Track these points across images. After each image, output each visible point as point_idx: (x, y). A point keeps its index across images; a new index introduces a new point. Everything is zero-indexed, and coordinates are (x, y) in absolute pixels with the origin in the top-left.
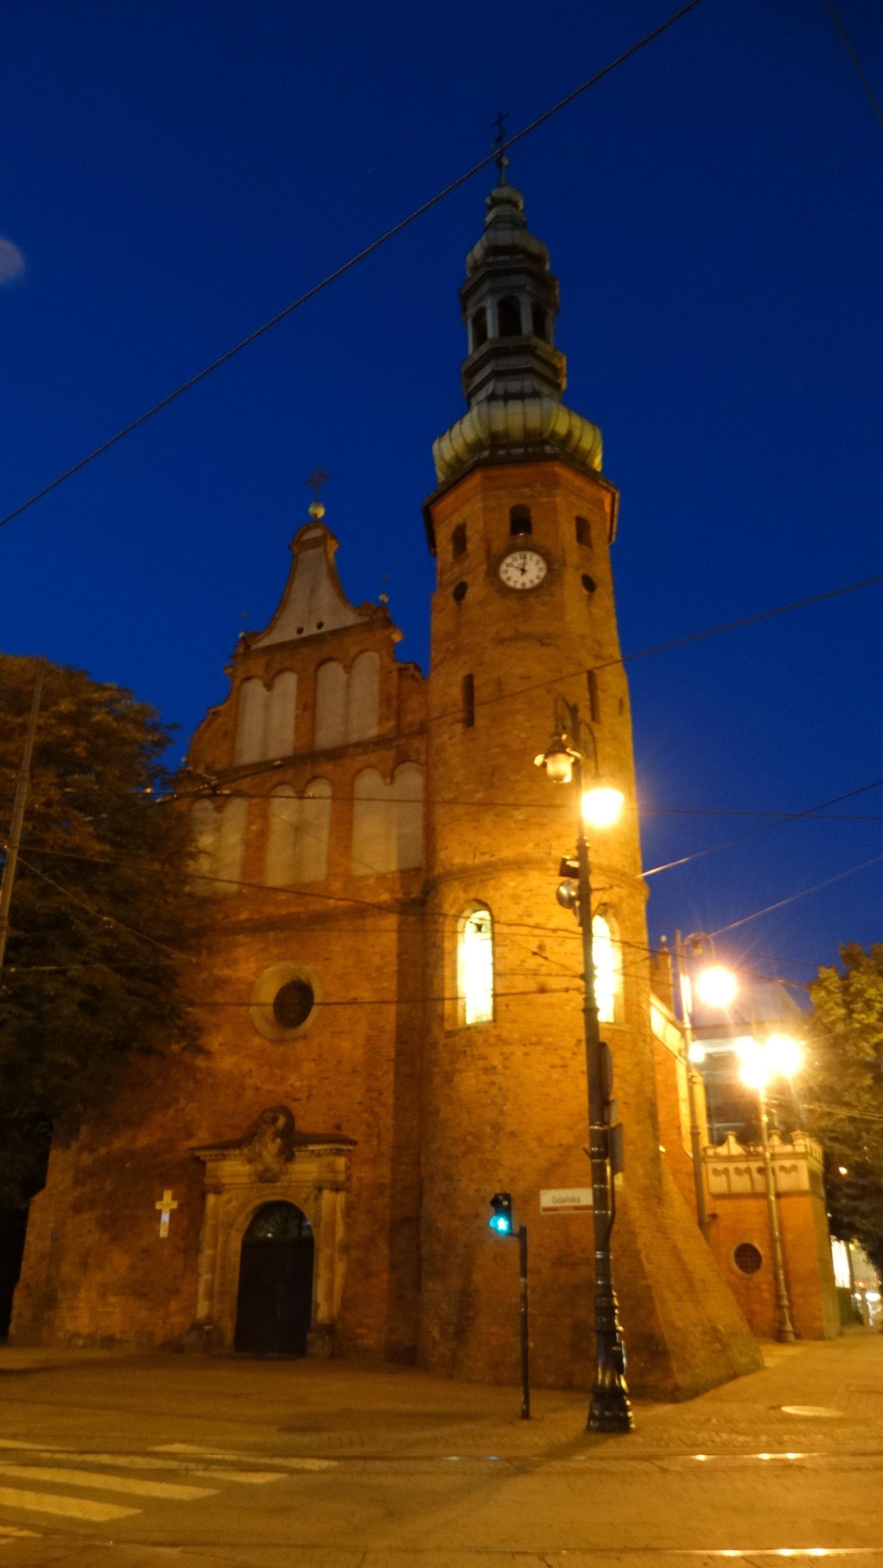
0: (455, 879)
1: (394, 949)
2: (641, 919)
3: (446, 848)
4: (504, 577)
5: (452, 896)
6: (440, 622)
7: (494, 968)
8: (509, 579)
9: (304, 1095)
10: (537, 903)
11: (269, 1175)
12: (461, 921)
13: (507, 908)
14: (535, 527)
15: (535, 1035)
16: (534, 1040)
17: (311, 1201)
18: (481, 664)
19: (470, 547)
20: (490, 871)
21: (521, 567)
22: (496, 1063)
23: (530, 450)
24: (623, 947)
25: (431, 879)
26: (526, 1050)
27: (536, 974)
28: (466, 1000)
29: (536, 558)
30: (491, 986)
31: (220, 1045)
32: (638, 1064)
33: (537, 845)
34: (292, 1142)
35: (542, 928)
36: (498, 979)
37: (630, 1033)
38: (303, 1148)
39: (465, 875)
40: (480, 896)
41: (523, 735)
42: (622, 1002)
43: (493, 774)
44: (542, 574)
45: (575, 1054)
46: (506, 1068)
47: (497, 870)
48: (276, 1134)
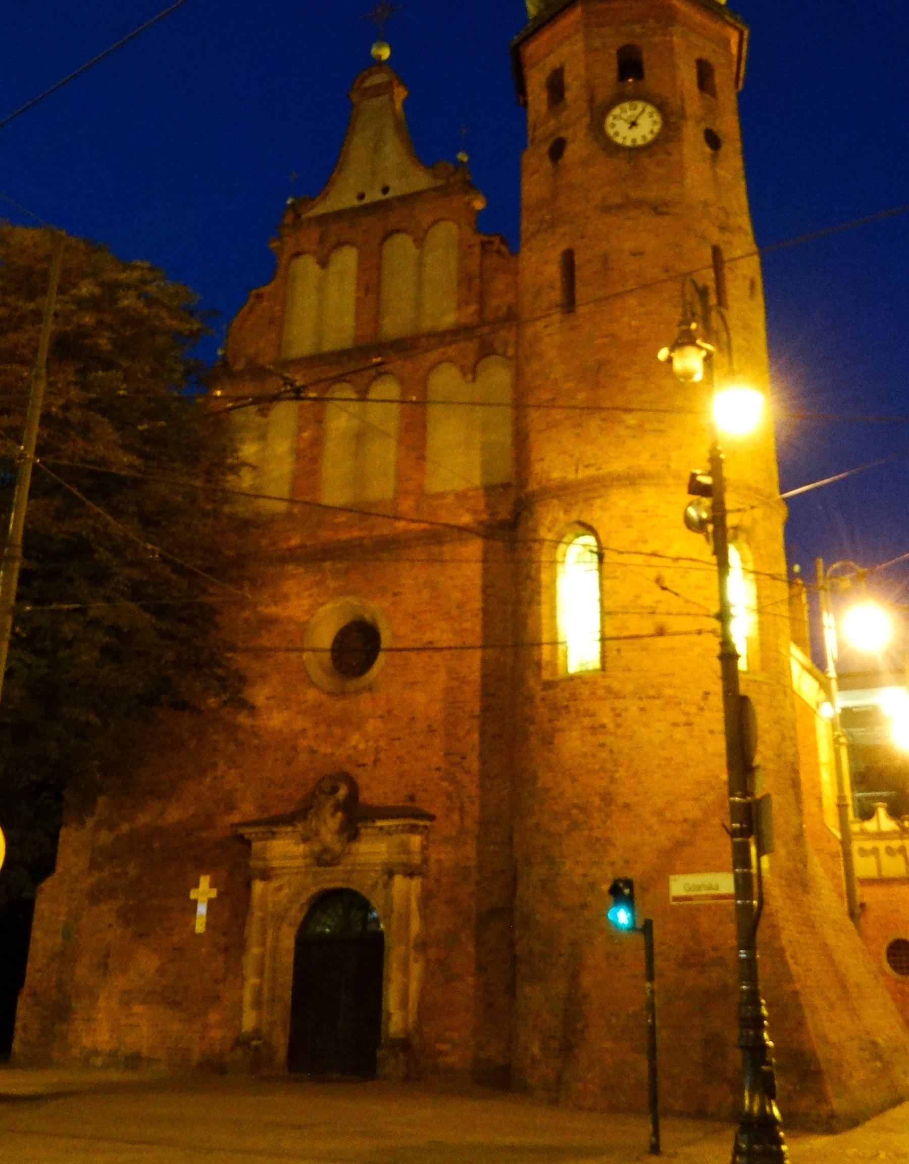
0: (553, 497)
4: (610, 131)
5: (550, 518)
6: (533, 185)
7: (602, 606)
9: (369, 760)
11: (328, 857)
12: (562, 547)
14: (647, 71)
15: (653, 686)
17: (380, 886)
19: (568, 95)
21: (633, 119)
25: (523, 496)
26: (641, 704)
27: (653, 613)
28: (568, 645)
30: (598, 627)
31: (267, 698)
32: (777, 721)
34: (356, 816)
35: (660, 556)
36: (607, 618)
37: (767, 684)
38: (369, 824)
39: (565, 492)
42: (756, 646)
43: (598, 371)
45: (701, 709)
47: (605, 486)
48: (337, 807)
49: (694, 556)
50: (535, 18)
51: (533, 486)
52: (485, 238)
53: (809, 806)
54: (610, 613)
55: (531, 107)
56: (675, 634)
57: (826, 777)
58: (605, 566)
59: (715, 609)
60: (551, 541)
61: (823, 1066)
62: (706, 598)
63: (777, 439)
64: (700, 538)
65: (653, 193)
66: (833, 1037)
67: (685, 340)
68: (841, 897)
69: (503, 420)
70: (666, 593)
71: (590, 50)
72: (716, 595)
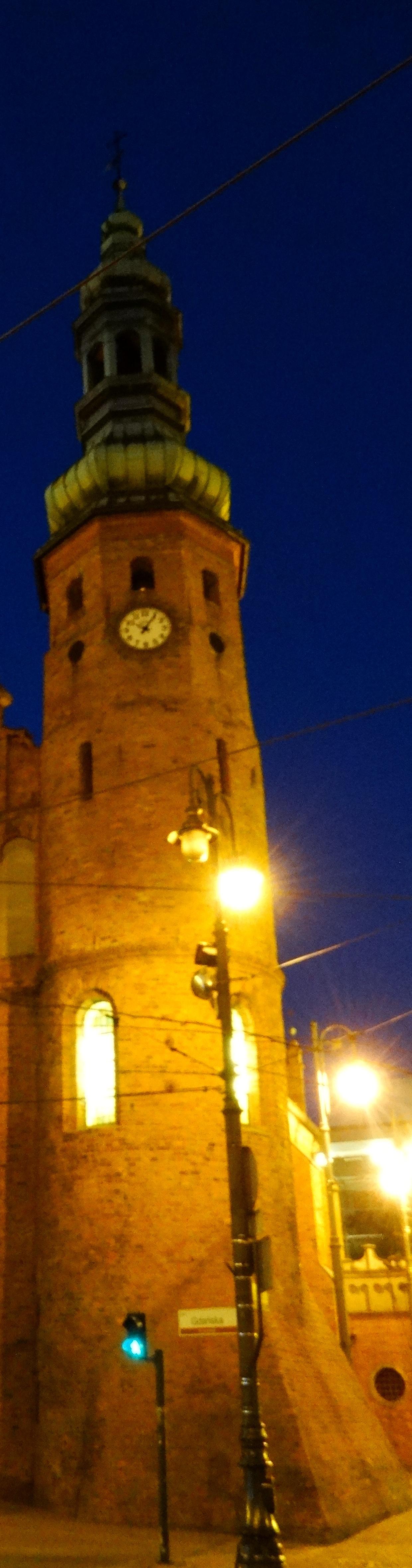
0: (73, 967)
2: (276, 1011)
3: (62, 933)
4: (124, 636)
5: (70, 985)
8: (130, 638)
10: (164, 993)
12: (80, 1012)
13: (130, 999)
15: (164, 1138)
16: (162, 1143)
18: (99, 731)
20: (112, 957)
21: (145, 625)
23: (153, 498)
24: (258, 1043)
29: (160, 615)
32: (275, 1171)
33: (163, 929)
35: (171, 1020)
36: (122, 1076)
41: (147, 809)
42: (257, 1101)
43: (113, 851)
44: (166, 633)
45: (208, 1159)
47: (119, 957)
49: (201, 1020)
50: (56, 534)
51: (54, 957)
52: (11, 733)
53: (305, 1247)
54: (124, 1072)
55: (52, 614)
56: (185, 1090)
57: (320, 1220)
58: (120, 1029)
59: (219, 1069)
60: (71, 1006)
61: (318, 1484)
62: (211, 1059)
63: (275, 912)
64: (205, 1004)
65: (162, 690)
66: (327, 1458)
67: (192, 825)
68: (333, 1328)
69: (28, 893)
70: (174, 1053)
71: (105, 562)
72: (221, 1056)
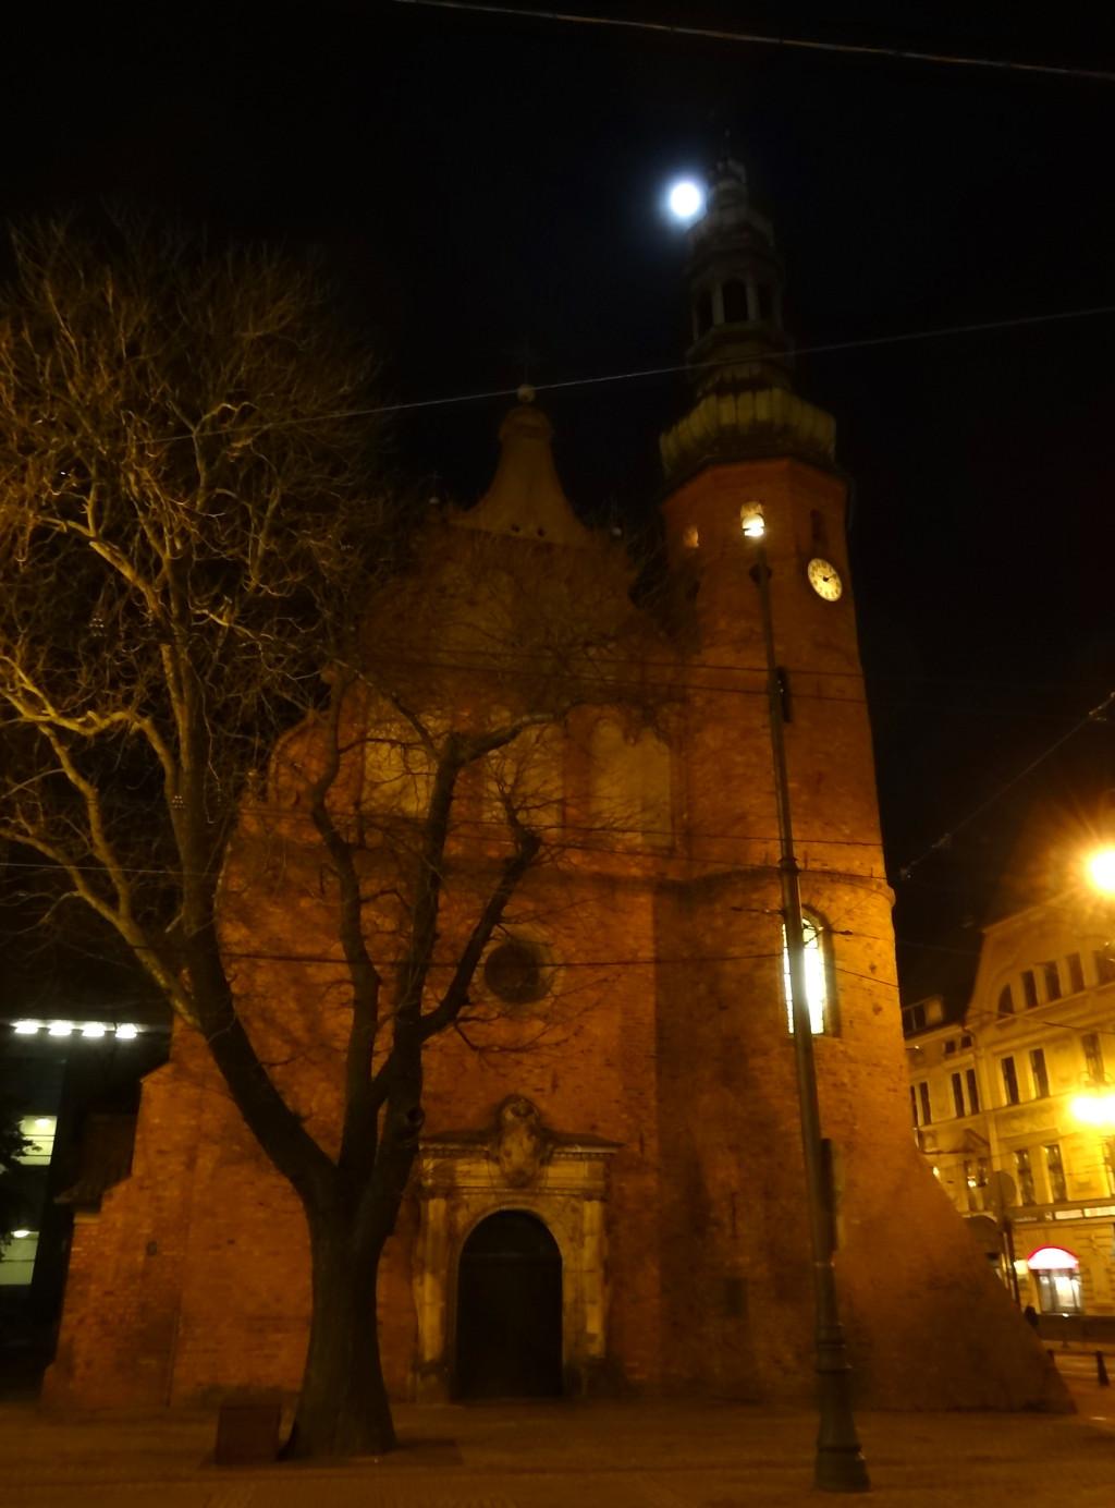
1: (650, 933)
22: (846, 1080)
34: (549, 1141)
40: (813, 904)
46: (855, 1086)
